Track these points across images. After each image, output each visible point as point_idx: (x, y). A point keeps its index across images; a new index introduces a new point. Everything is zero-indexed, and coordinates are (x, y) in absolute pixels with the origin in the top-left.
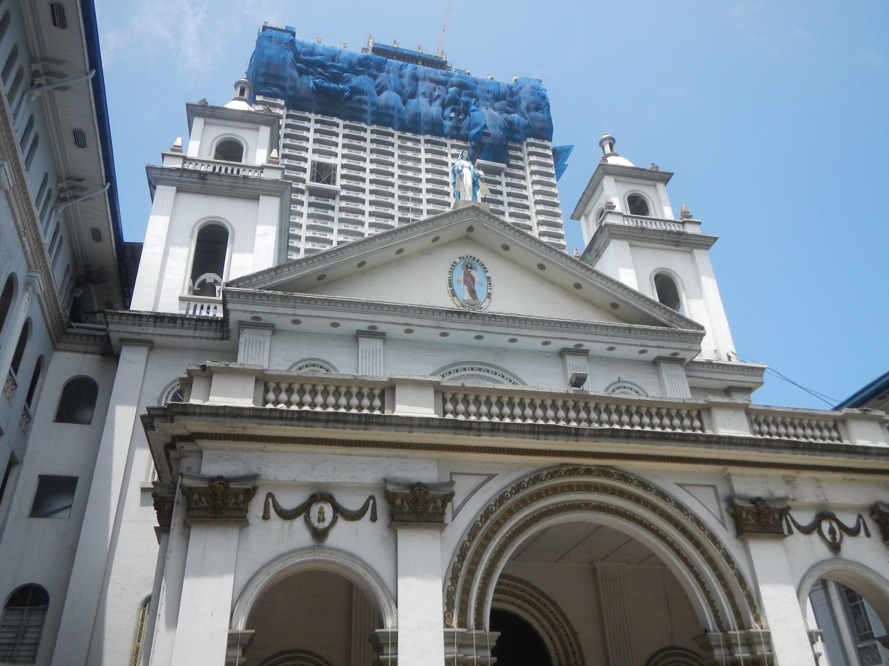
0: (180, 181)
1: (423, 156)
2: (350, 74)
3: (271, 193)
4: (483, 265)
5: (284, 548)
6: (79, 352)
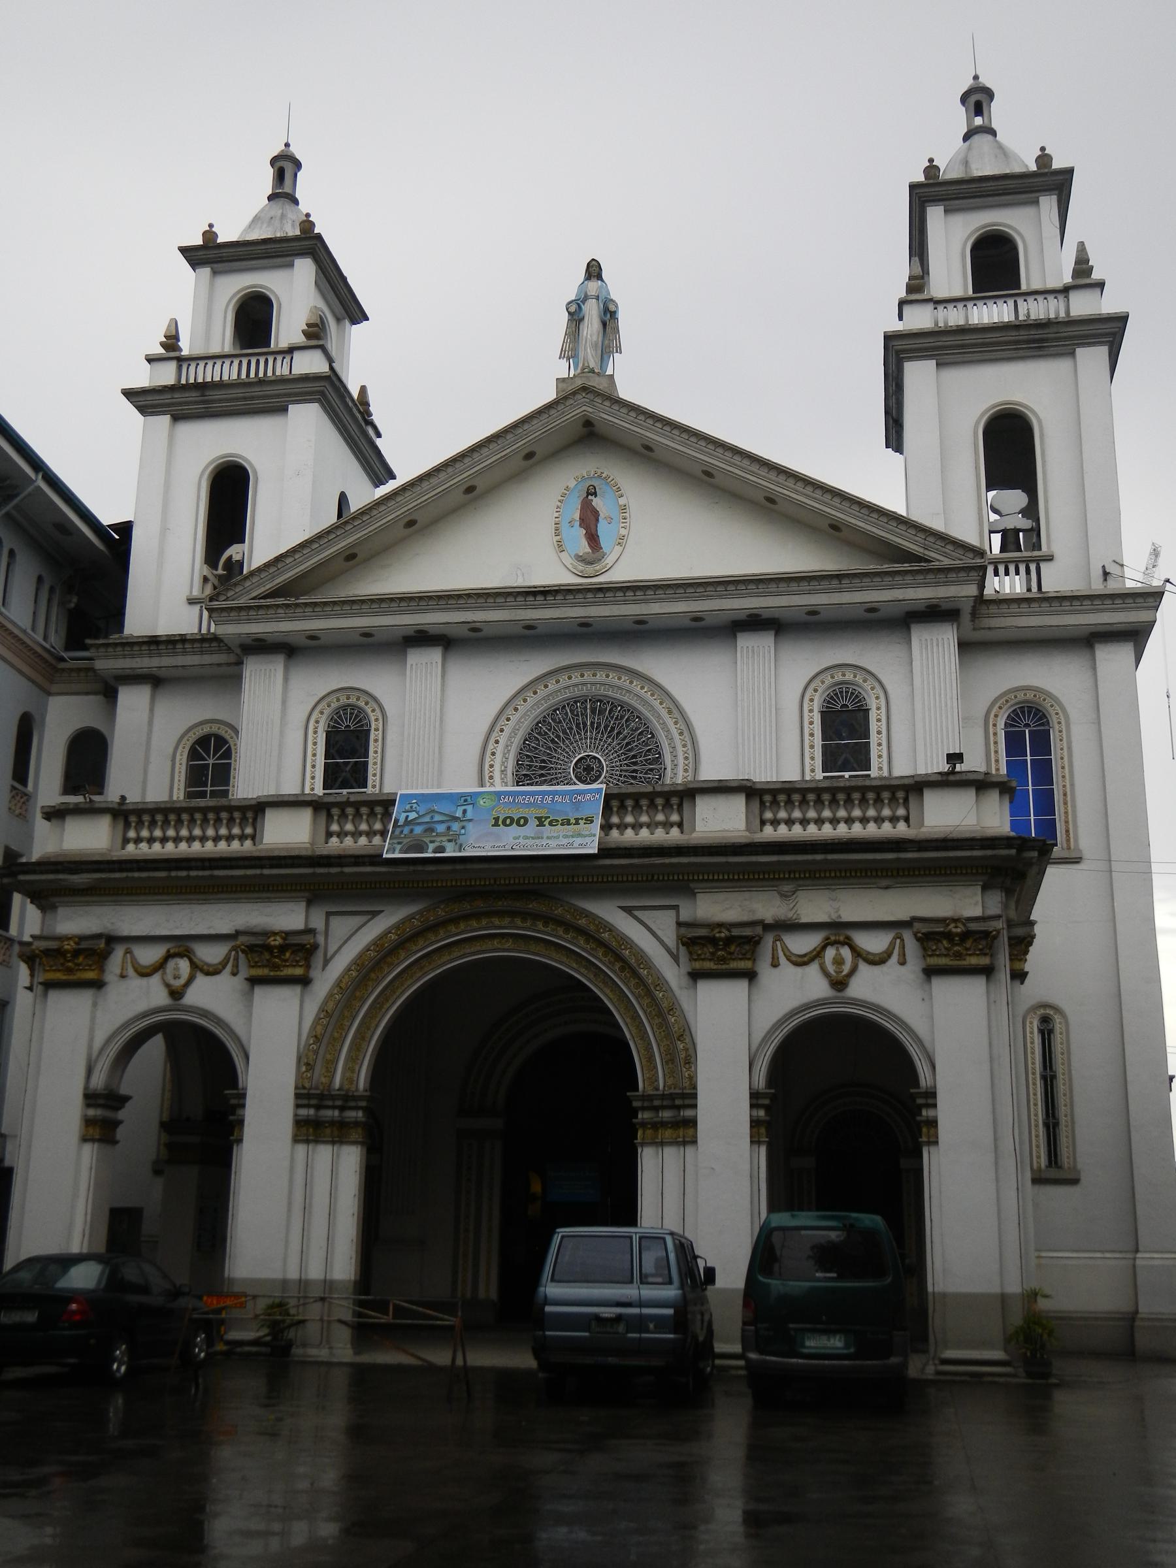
3: (303, 398)
5: (142, 1006)
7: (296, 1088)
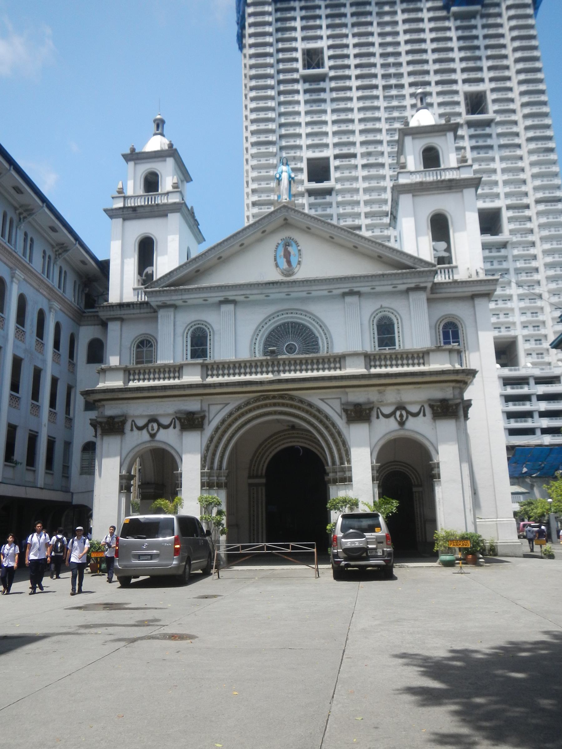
0: (123, 214)
1: (400, 17)
4: (296, 242)
5: (140, 441)
6: (91, 325)
7: (201, 470)
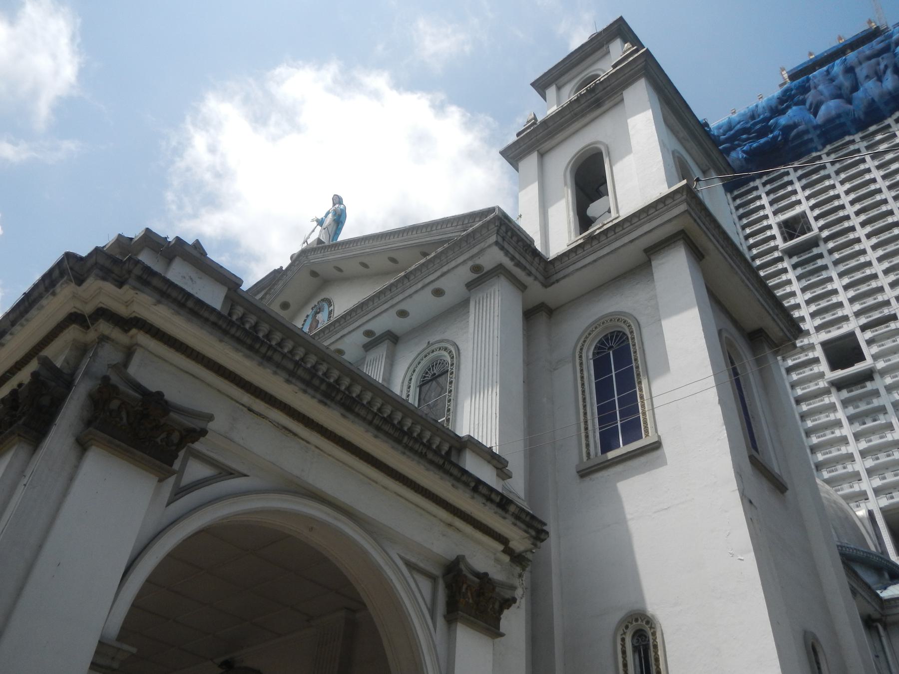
2: (775, 119)
